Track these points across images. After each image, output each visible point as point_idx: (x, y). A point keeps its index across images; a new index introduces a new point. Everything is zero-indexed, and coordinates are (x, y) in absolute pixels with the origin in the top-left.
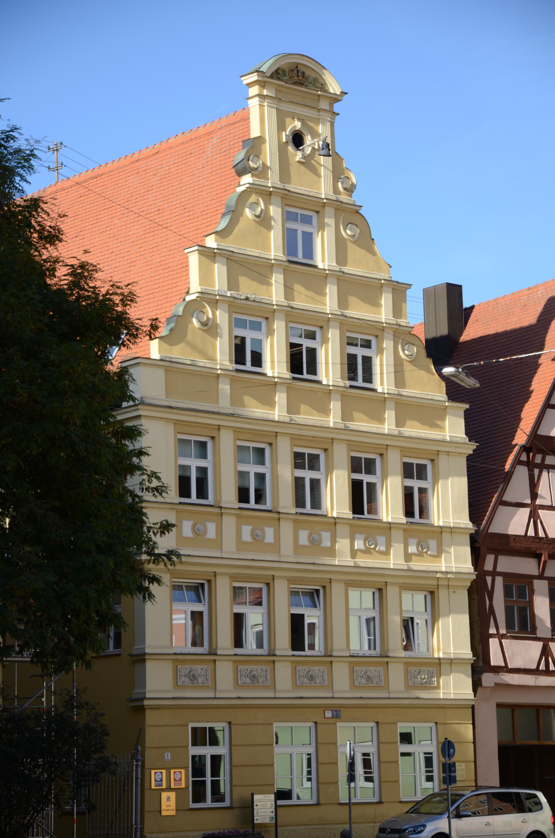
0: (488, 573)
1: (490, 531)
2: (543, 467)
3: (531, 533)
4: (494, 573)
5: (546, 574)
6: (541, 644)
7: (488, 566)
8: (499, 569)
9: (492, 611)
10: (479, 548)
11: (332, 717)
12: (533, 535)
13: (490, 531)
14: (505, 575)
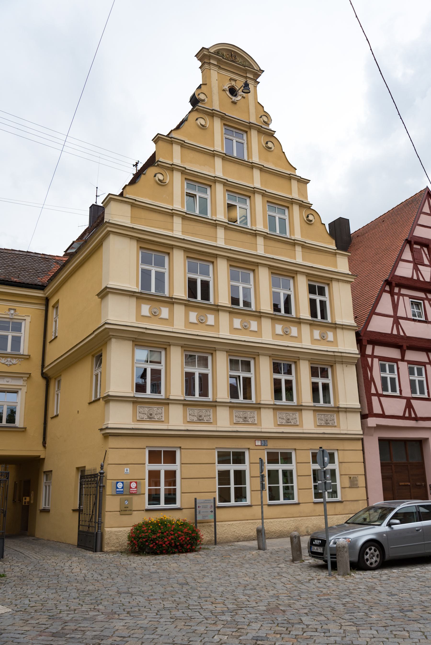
0: (369, 356)
1: (369, 329)
2: (399, 294)
3: (395, 332)
4: (373, 356)
5: (406, 358)
6: (405, 401)
7: (369, 351)
8: (375, 354)
9: (372, 379)
10: (361, 340)
11: (261, 445)
12: (396, 334)
13: (369, 329)
14: (381, 359)
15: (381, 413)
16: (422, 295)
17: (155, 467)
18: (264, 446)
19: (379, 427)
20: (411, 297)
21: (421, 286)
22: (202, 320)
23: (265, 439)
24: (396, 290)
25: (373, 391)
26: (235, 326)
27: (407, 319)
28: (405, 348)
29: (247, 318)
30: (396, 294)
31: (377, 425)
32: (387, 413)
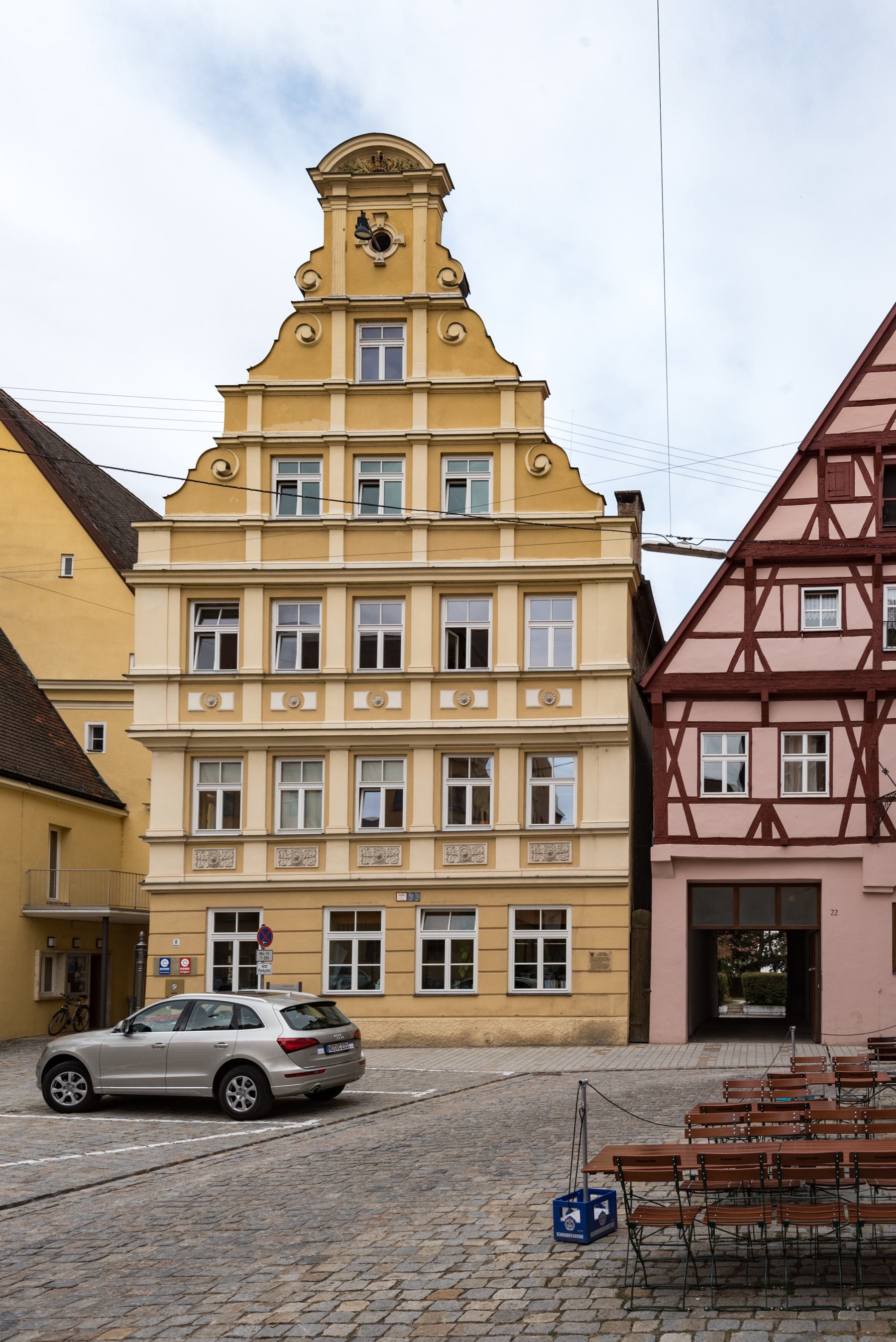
3: (740, 667)
9: (675, 770)
15: (688, 833)
16: (844, 572)
17: (224, 937)
18: (413, 901)
19: (675, 860)
20: (802, 583)
21: (831, 554)
22: (294, 703)
23: (414, 891)
24: (763, 574)
25: (674, 792)
26: (356, 706)
27: (782, 634)
28: (765, 697)
29: (381, 688)
30: (762, 583)
31: (672, 857)
32: (701, 834)
